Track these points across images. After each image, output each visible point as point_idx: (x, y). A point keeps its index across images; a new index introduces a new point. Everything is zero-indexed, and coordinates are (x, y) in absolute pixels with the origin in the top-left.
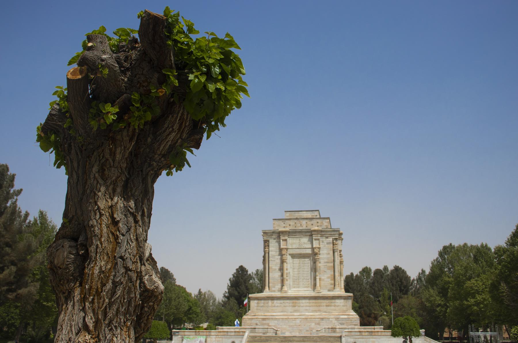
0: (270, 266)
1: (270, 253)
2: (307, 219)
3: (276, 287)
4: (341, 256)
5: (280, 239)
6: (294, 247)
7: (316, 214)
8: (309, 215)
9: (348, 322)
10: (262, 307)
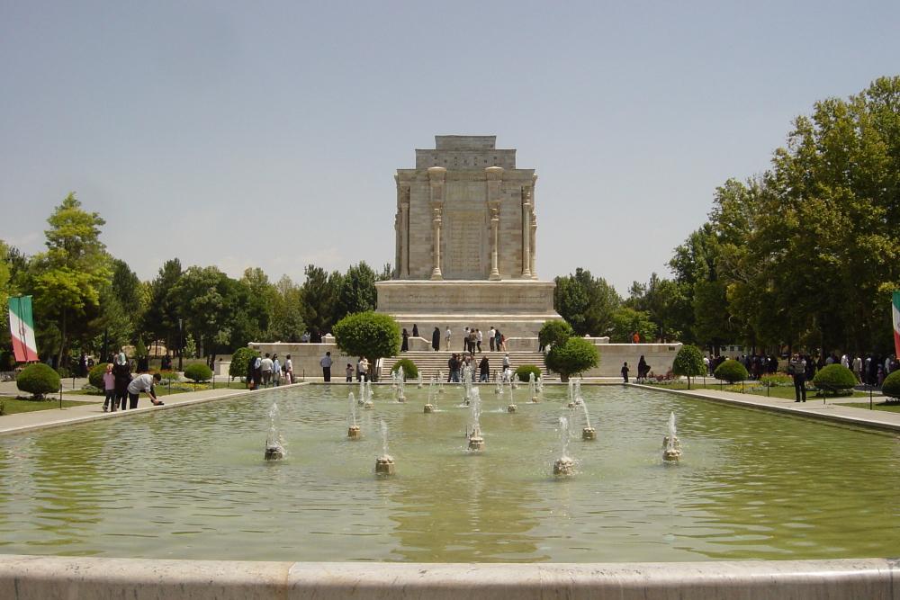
0: (411, 232)
1: (411, 210)
2: (476, 150)
3: (422, 268)
4: (533, 218)
5: (429, 185)
7: (491, 143)
8: (479, 145)
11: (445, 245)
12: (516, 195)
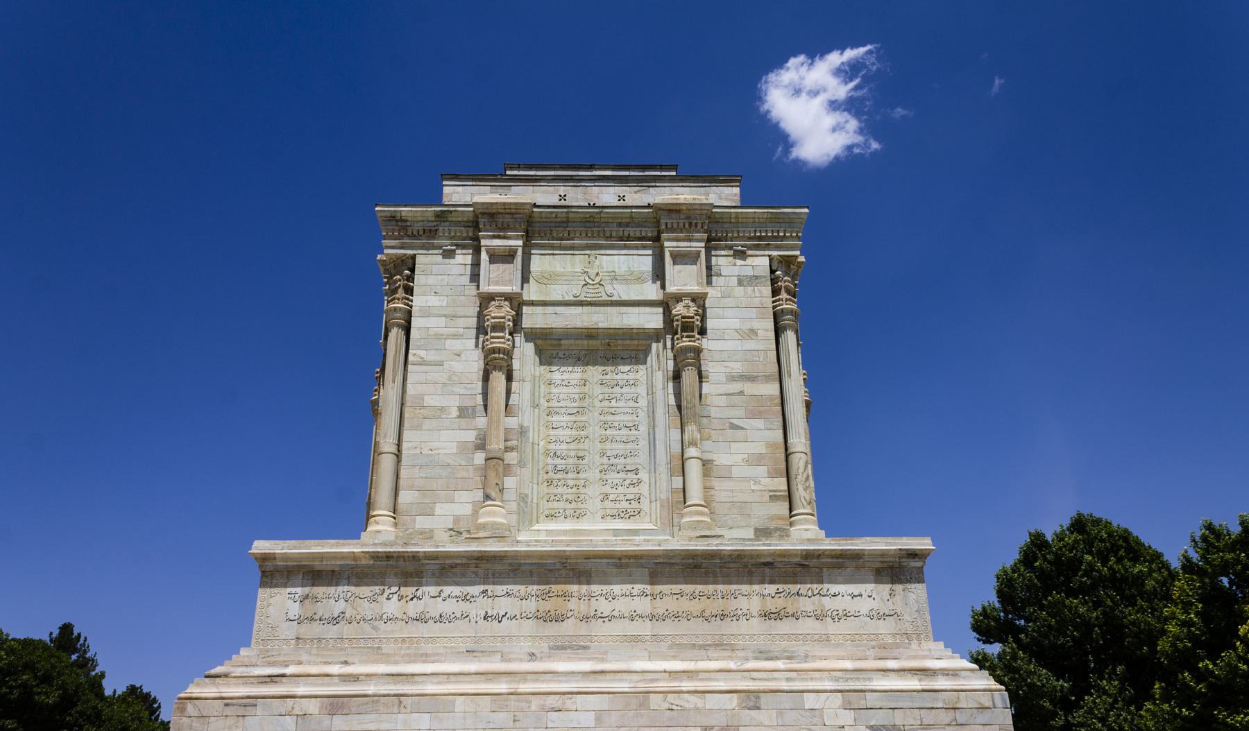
6: (557, 293)
9: (929, 717)
10: (335, 620)
11: (522, 431)
12: (753, 280)
